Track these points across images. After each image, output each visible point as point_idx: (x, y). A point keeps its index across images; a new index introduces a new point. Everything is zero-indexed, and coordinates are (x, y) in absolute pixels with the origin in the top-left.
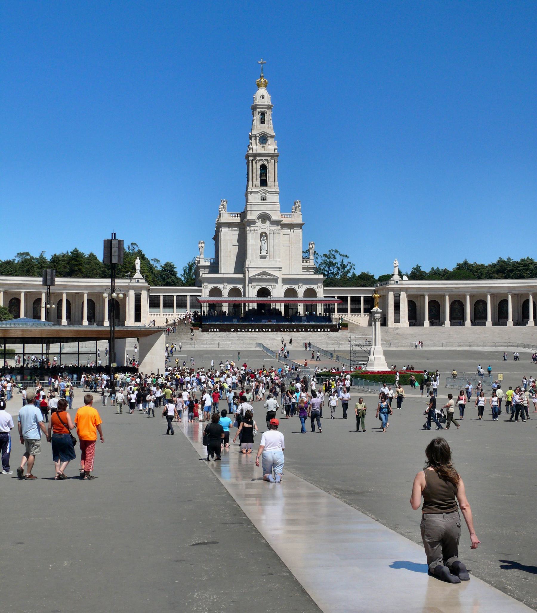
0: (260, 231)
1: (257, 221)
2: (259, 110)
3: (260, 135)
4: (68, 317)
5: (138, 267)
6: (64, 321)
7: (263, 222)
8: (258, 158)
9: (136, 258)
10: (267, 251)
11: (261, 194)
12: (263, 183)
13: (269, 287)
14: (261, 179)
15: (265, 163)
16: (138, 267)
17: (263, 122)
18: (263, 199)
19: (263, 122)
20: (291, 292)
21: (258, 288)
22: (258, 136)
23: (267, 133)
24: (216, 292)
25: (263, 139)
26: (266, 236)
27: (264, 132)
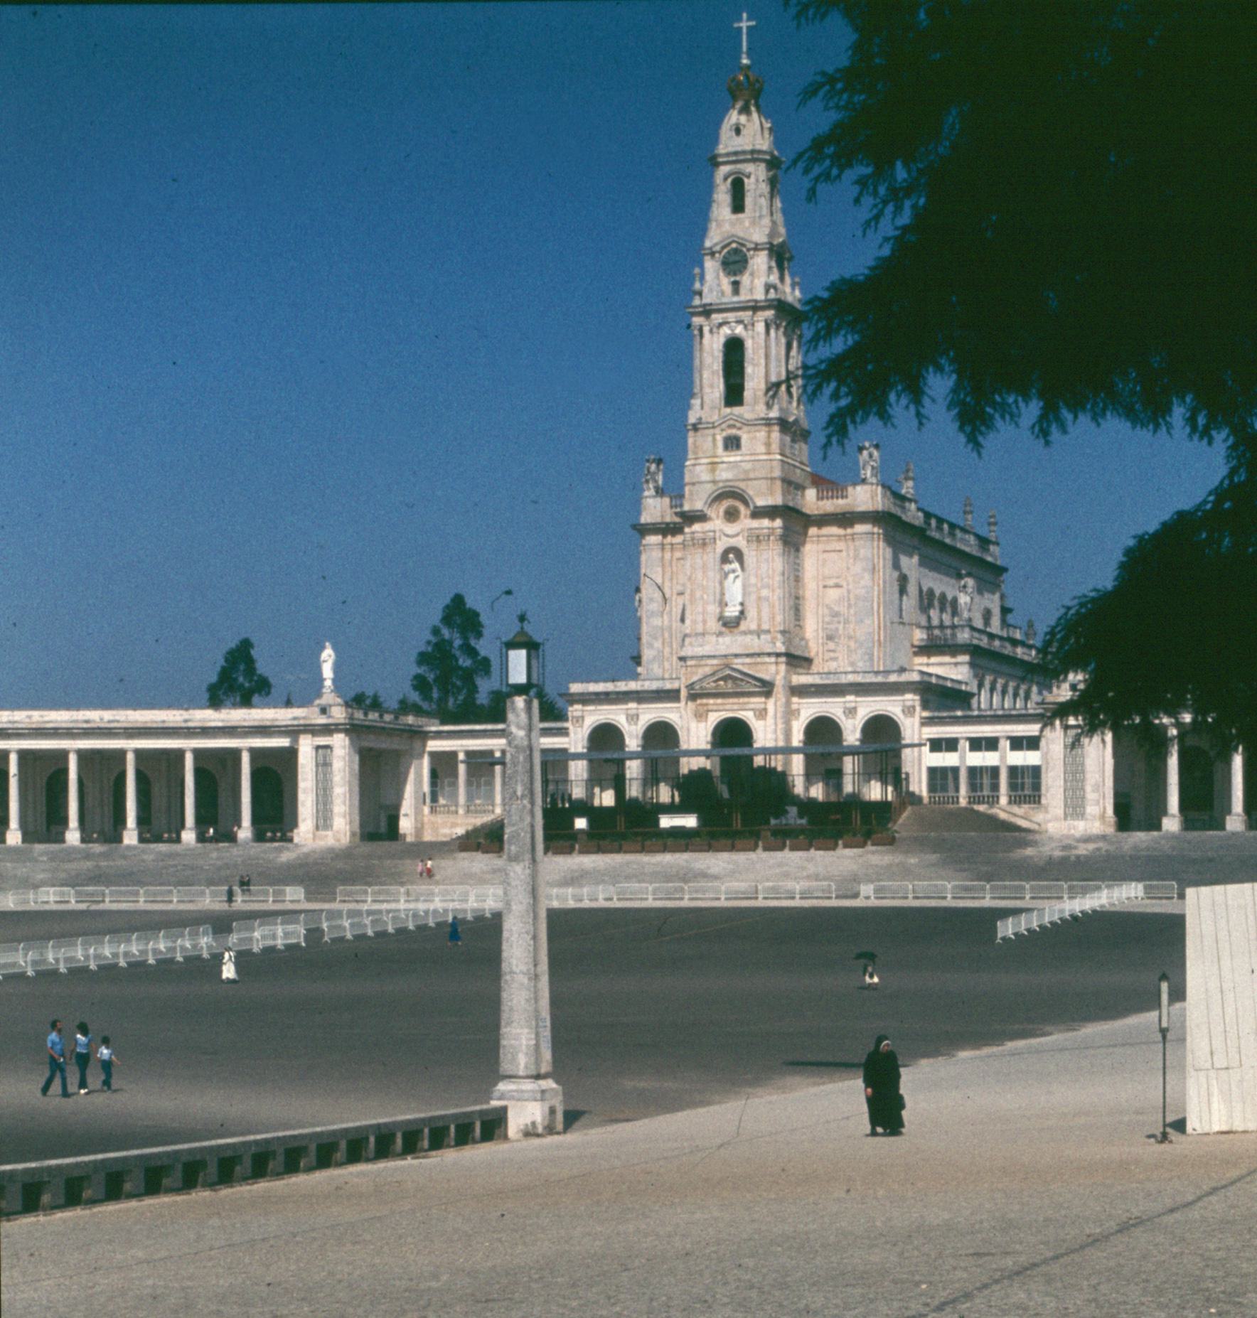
0: (721, 546)
1: (710, 513)
2: (724, 170)
3: (723, 248)
4: (142, 821)
5: (327, 671)
6: (130, 837)
7: (731, 515)
8: (717, 318)
9: (323, 648)
10: (742, 604)
11: (722, 430)
12: (734, 394)
13: (748, 716)
14: (732, 381)
15: (739, 330)
16: (327, 671)
17: (738, 206)
18: (733, 443)
19: (738, 206)
20: (822, 730)
21: (714, 718)
22: (720, 252)
23: (746, 240)
24: (606, 737)
25: (735, 262)
26: (739, 555)
27: (733, 236)
